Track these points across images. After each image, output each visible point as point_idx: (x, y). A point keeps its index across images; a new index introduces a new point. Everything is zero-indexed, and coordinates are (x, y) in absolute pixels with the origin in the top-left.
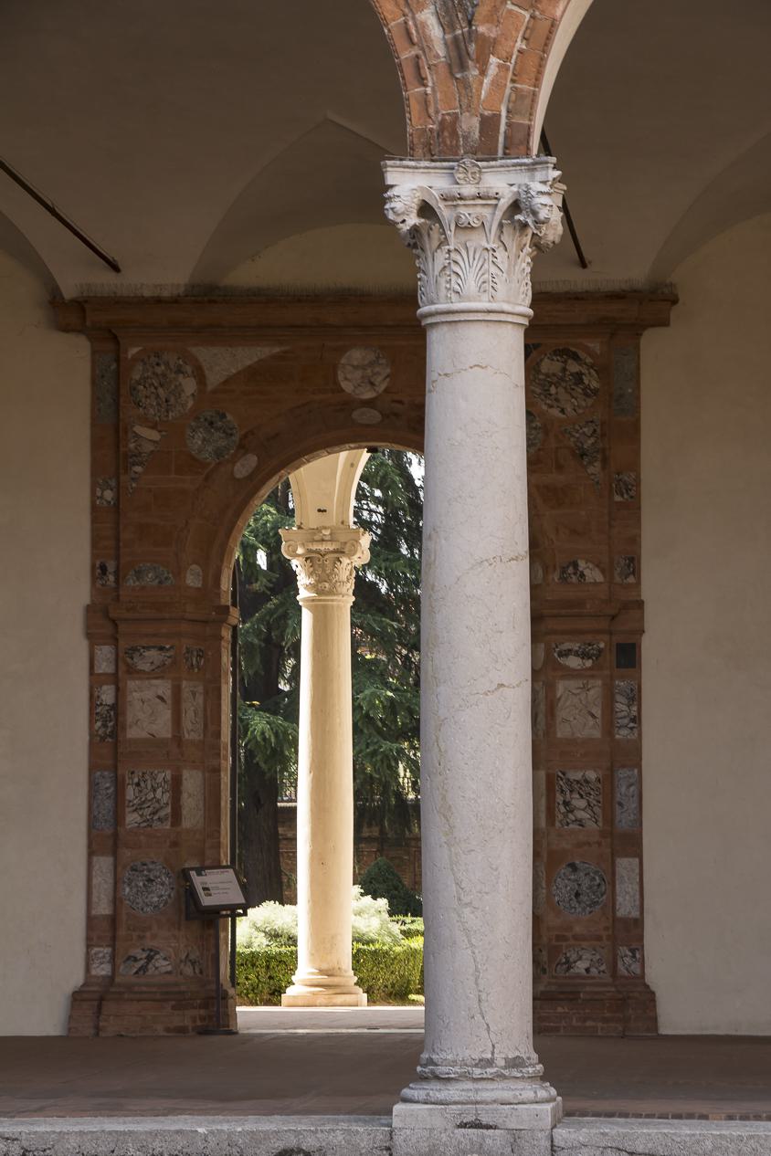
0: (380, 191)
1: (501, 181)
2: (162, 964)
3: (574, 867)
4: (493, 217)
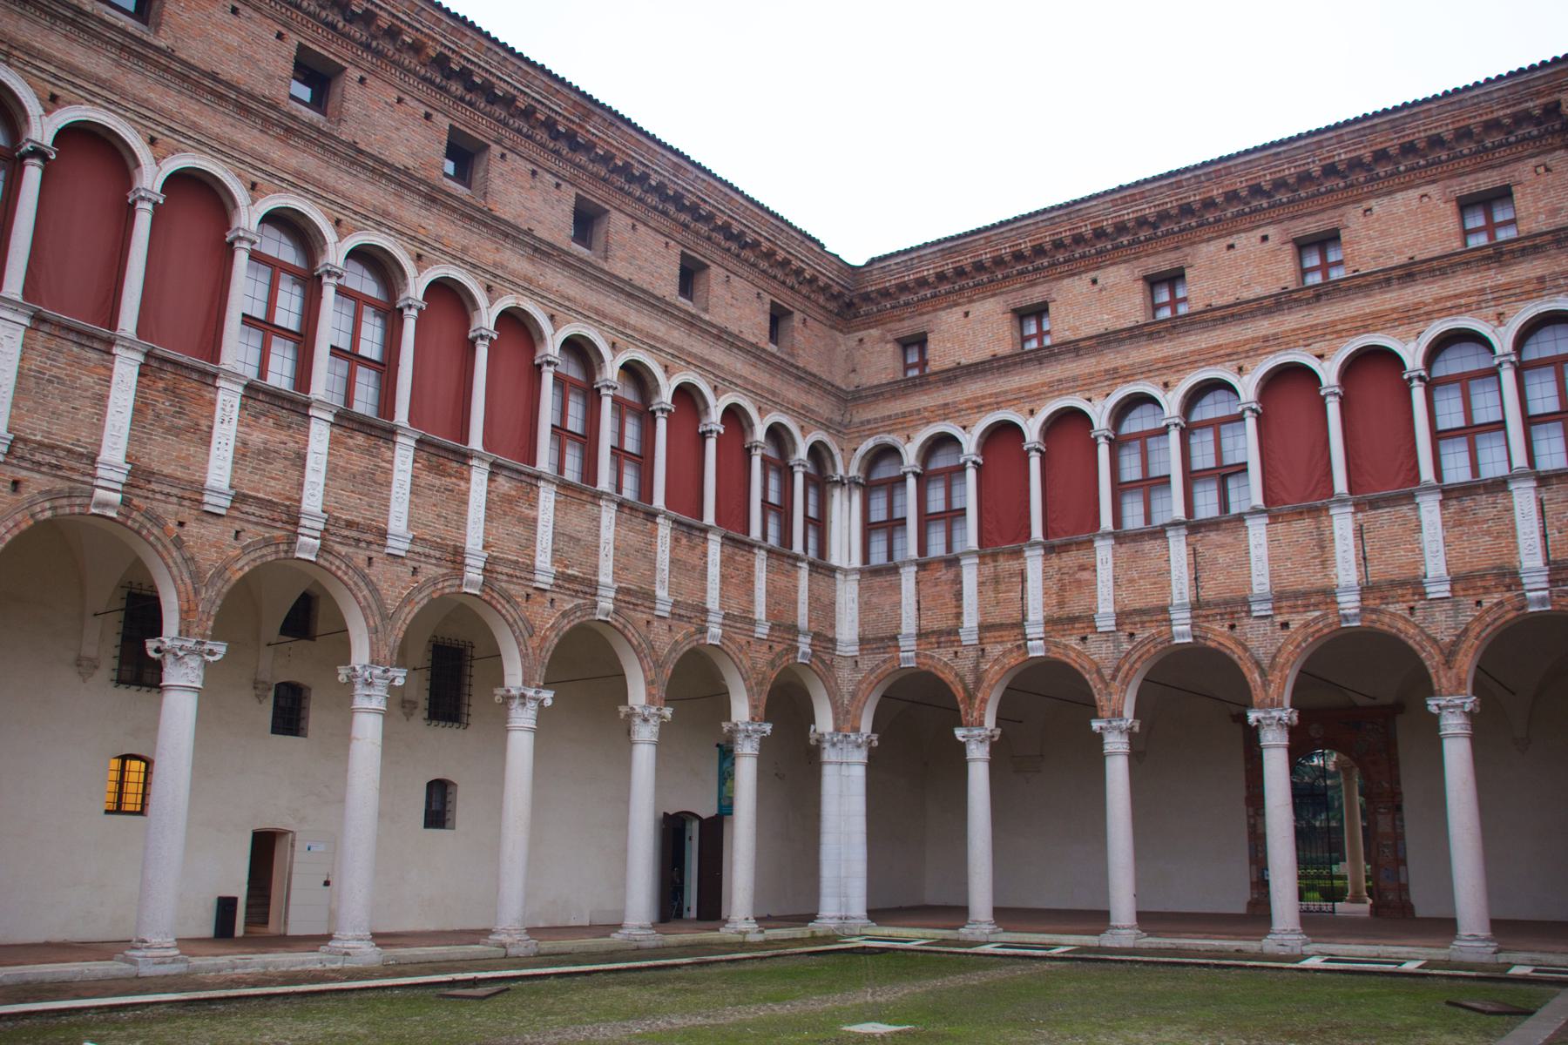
0: (1246, 717)
1: (1276, 714)
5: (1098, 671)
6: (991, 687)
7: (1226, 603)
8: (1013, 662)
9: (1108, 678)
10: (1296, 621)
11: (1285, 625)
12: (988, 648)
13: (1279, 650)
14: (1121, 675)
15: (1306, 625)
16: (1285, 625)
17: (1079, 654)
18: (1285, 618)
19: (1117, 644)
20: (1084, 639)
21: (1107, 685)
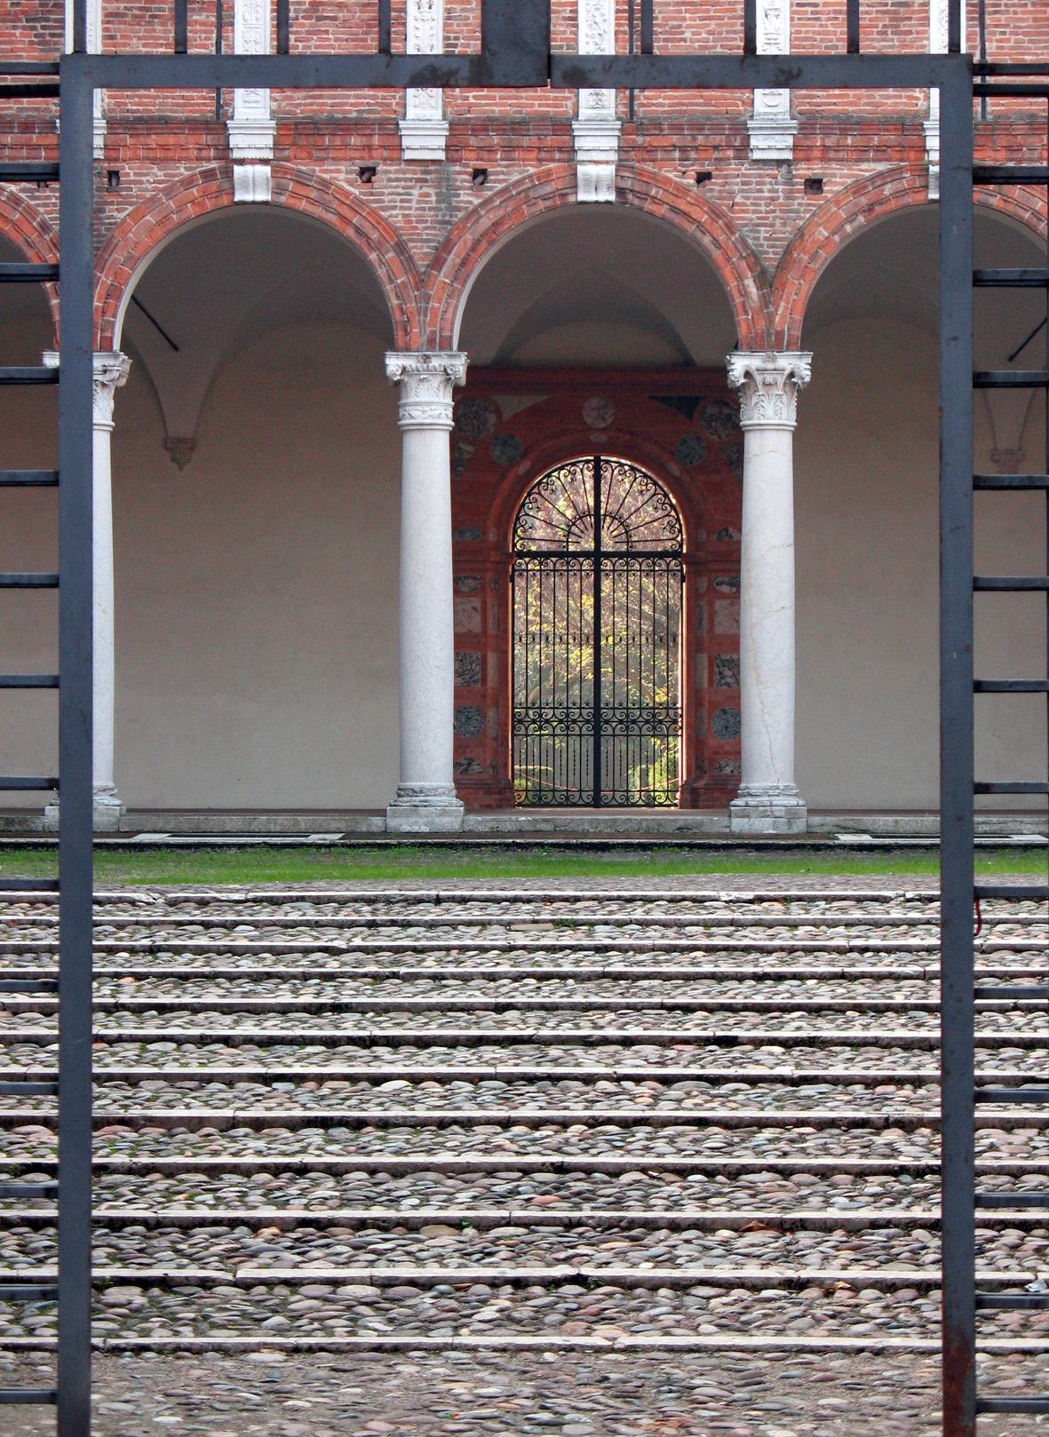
2: (476, 768)
3: (725, 712)
4: (781, 380)
5: (401, 248)
6: (132, 261)
7: (697, 127)
8: (191, 210)
9: (422, 264)
10: (839, 177)
11: (815, 185)
12: (128, 171)
13: (800, 233)
14: (452, 259)
15: (858, 188)
16: (815, 185)
17: (357, 206)
18: (815, 170)
19: (447, 193)
20: (367, 173)
21: (421, 282)
